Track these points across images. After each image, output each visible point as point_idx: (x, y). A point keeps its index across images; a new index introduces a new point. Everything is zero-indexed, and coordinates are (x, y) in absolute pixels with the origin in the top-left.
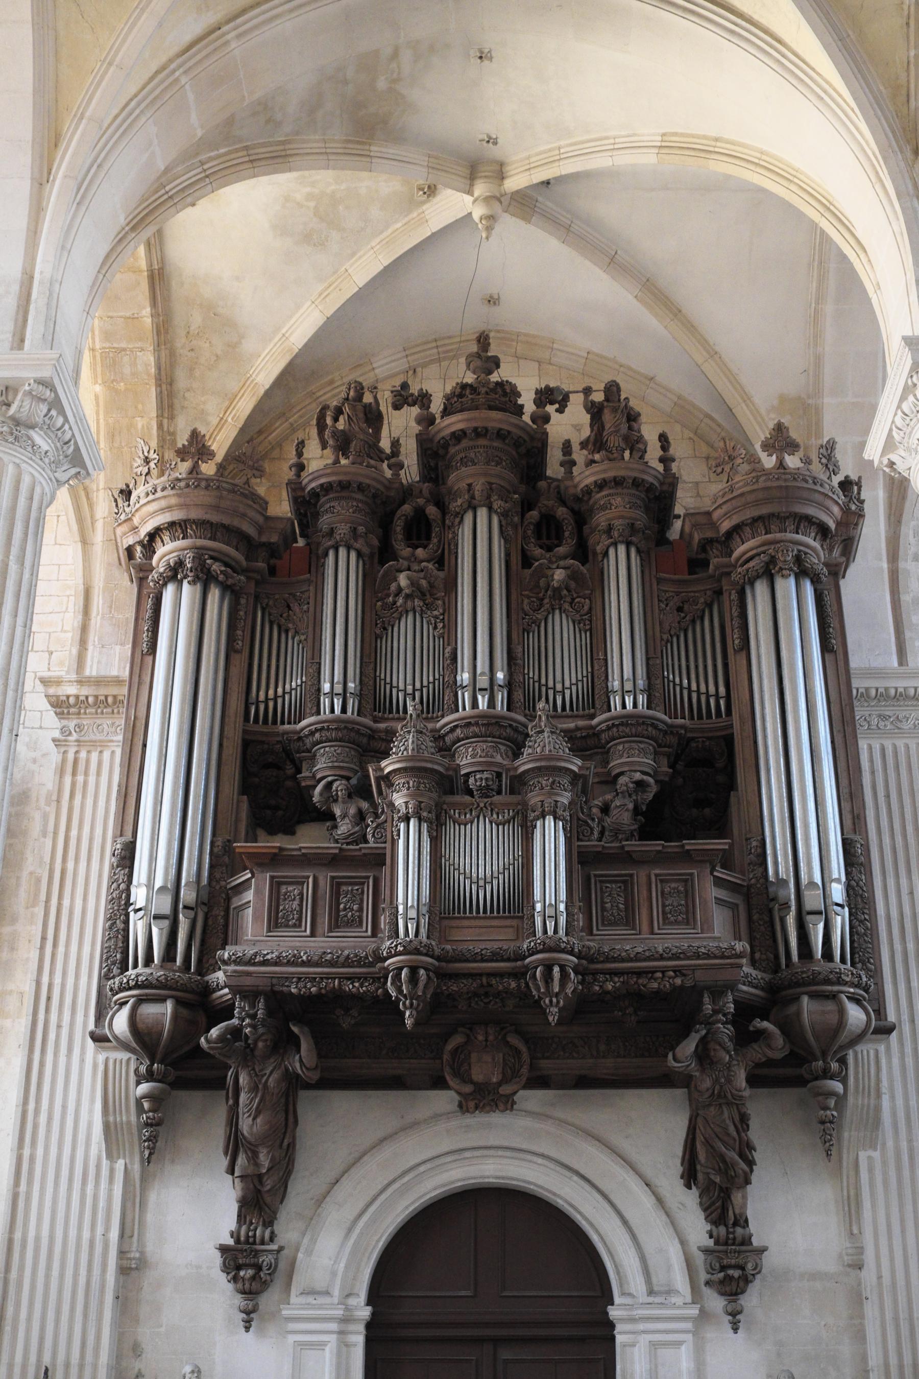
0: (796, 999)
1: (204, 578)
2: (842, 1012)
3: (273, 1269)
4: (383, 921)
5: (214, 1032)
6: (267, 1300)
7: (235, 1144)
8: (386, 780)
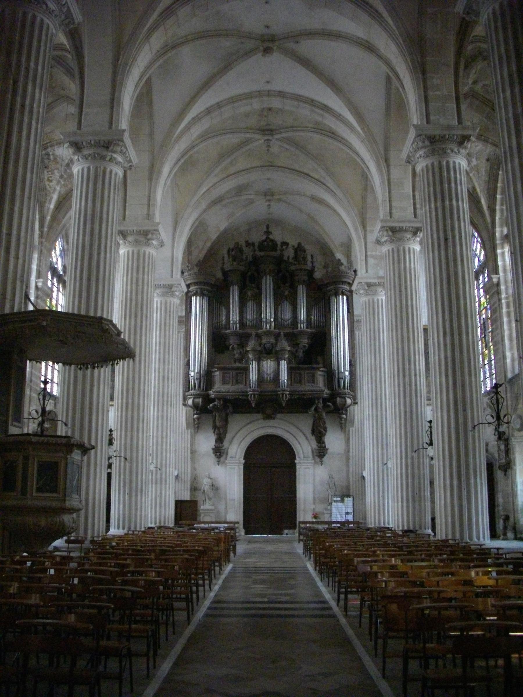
0: (336, 398)
1: (202, 295)
2: (346, 401)
3: (223, 453)
4: (247, 383)
5: (211, 405)
6: (222, 459)
7: (215, 427)
8: (248, 351)
